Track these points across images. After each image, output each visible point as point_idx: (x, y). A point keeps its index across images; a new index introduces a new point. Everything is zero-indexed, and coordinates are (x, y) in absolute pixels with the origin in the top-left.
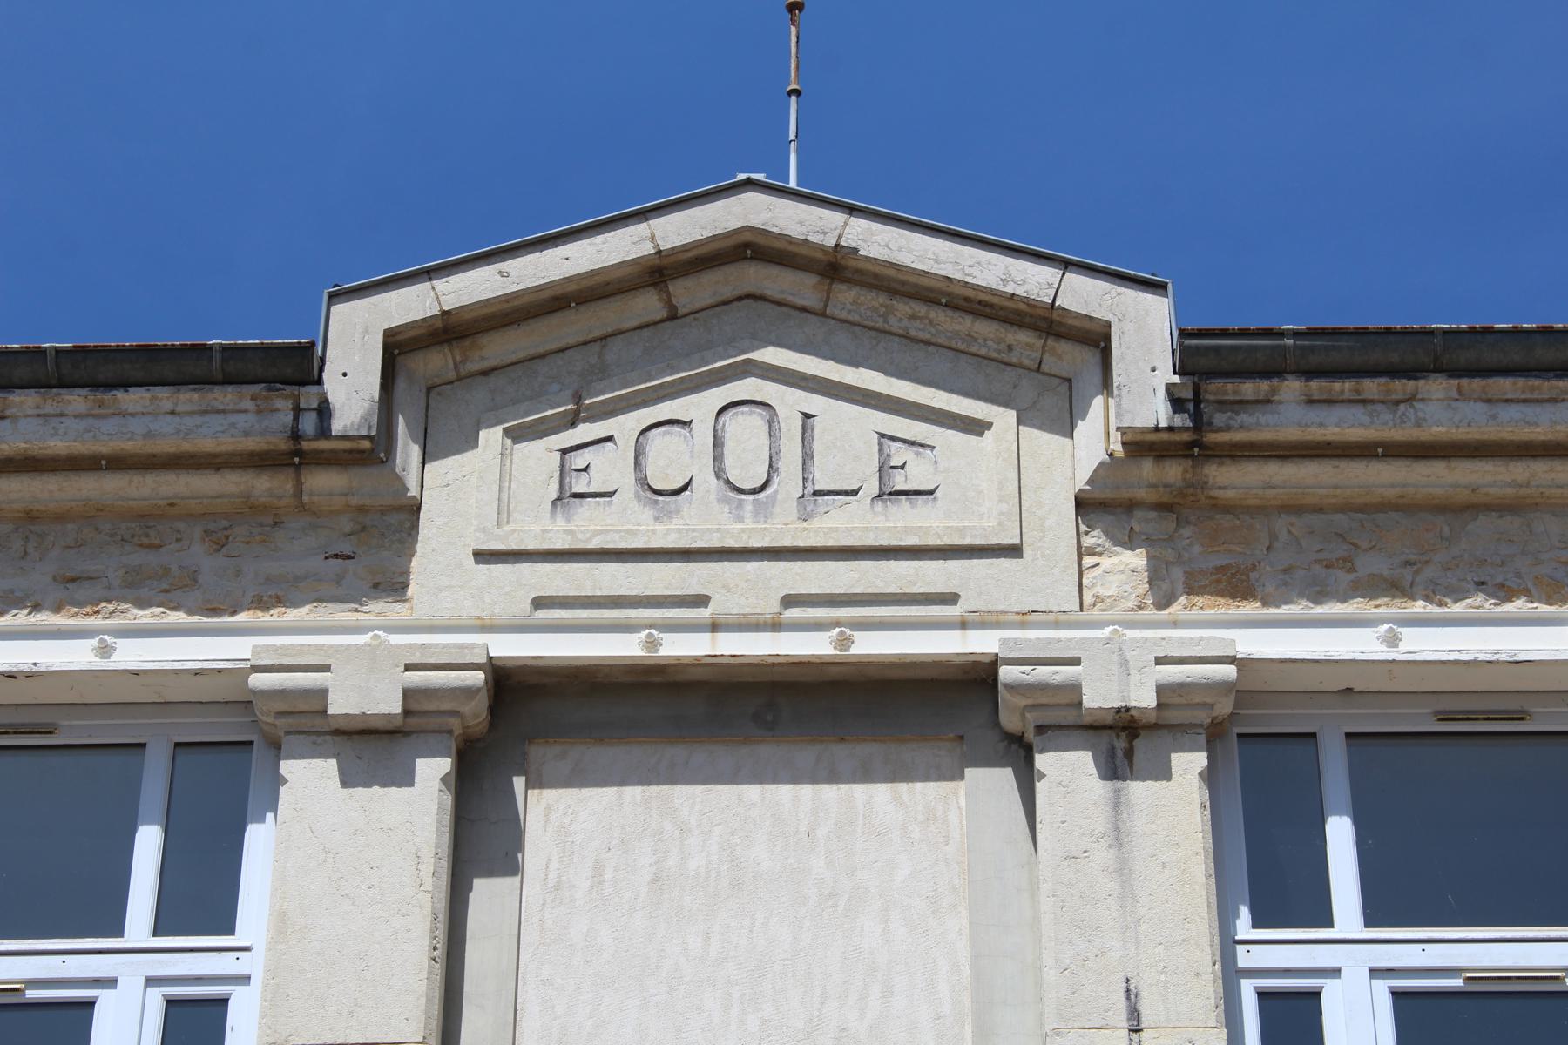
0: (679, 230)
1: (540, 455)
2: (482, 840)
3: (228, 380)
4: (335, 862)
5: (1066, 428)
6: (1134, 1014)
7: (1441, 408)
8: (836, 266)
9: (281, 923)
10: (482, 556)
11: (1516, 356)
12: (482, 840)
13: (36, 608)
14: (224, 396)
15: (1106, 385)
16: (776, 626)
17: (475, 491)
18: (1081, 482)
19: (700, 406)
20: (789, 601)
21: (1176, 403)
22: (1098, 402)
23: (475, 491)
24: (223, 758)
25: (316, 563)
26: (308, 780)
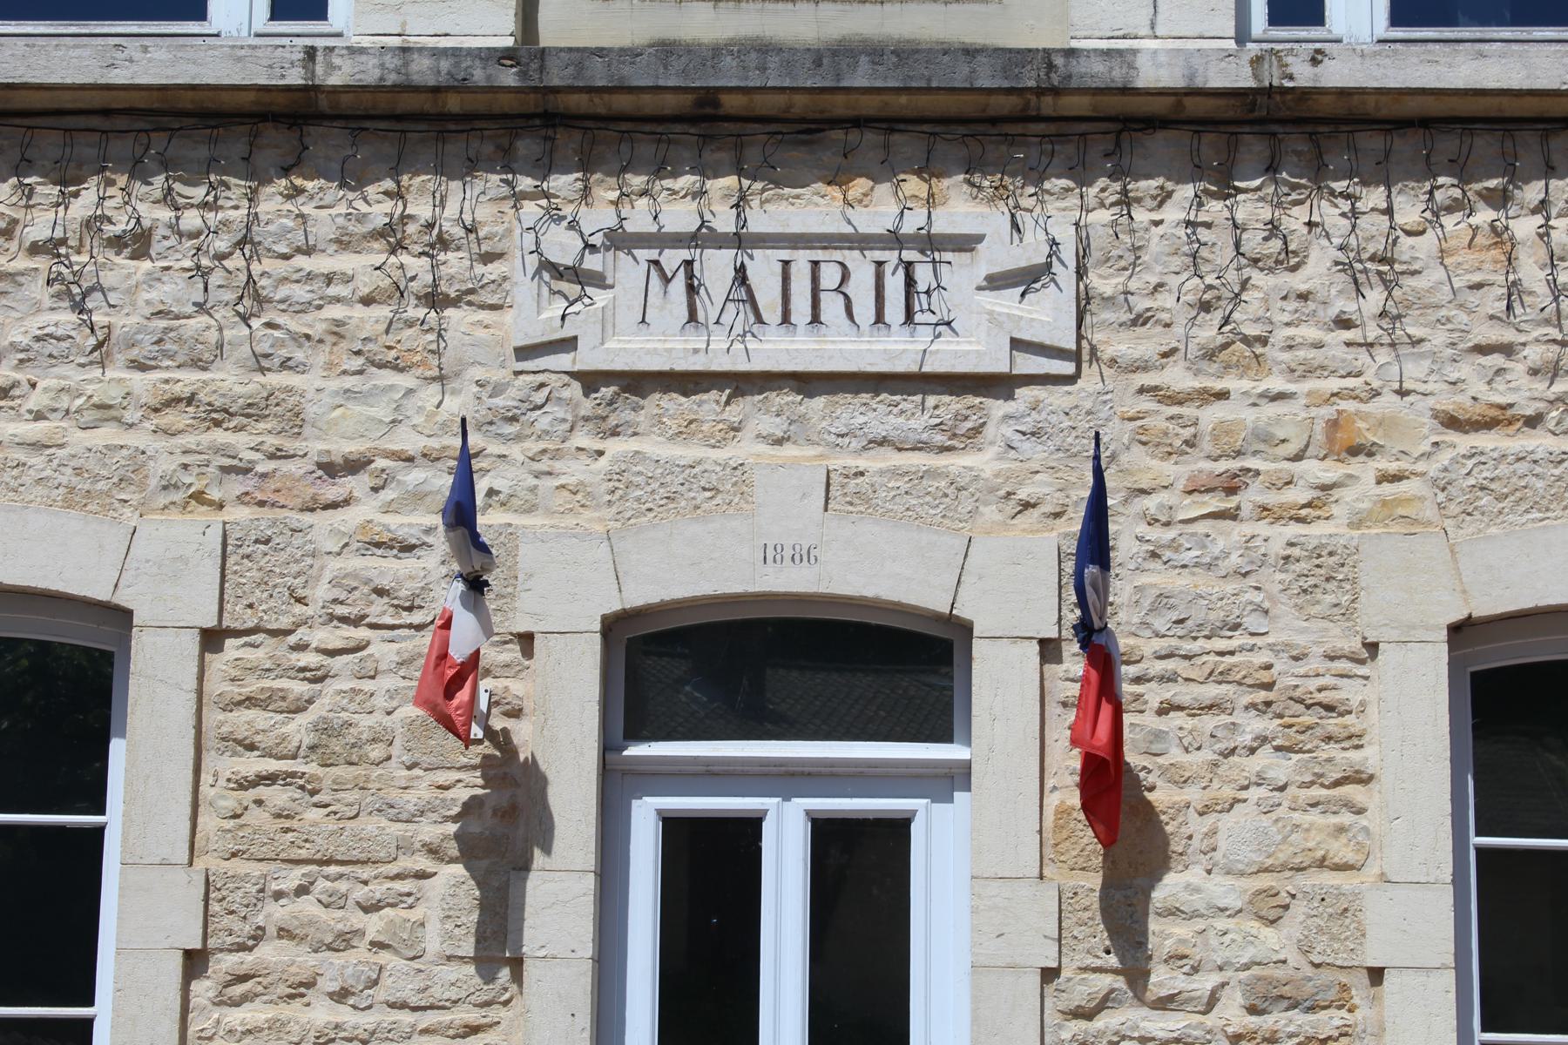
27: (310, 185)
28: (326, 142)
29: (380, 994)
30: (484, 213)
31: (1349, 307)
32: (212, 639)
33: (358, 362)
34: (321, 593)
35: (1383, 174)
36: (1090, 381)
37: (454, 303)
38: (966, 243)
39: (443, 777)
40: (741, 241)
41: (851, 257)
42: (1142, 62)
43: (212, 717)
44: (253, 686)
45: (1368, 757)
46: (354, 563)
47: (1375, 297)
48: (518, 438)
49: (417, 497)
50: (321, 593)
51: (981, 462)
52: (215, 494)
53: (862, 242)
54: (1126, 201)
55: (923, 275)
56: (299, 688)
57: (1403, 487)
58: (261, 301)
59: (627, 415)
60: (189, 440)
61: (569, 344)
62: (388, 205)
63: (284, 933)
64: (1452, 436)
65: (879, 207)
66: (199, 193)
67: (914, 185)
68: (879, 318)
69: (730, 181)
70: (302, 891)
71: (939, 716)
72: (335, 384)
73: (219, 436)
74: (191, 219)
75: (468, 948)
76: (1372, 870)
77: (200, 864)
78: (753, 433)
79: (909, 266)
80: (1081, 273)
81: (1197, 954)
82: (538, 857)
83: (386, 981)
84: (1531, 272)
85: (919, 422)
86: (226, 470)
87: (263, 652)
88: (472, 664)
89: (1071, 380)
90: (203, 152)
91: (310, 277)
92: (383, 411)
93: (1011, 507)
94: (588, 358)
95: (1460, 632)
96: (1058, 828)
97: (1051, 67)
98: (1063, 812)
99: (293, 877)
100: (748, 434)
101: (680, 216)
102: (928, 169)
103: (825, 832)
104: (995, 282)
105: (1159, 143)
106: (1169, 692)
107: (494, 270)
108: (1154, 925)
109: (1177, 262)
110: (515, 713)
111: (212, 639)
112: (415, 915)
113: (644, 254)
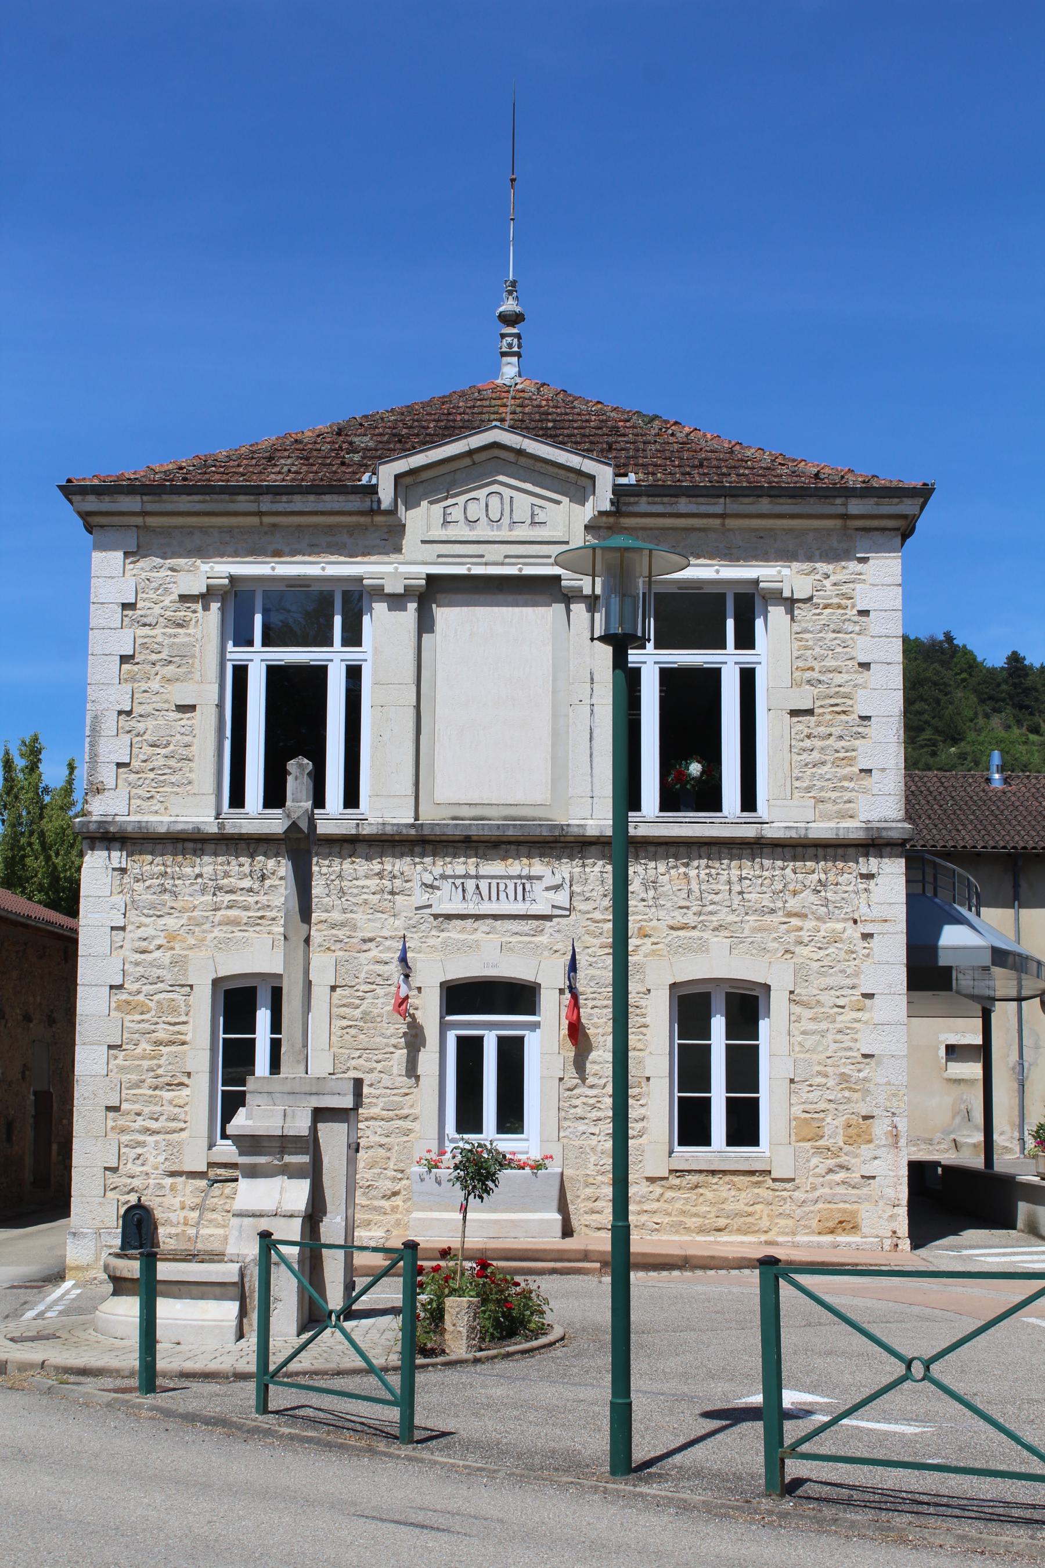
0: (476, 441)
1: (438, 508)
2: (425, 624)
4: (386, 629)
5: (582, 502)
6: (592, 679)
7: (684, 505)
8: (520, 452)
9: (375, 649)
10: (423, 542)
11: (705, 493)
12: (425, 624)
13: (304, 555)
14: (352, 497)
15: (594, 494)
16: (502, 564)
17: (421, 520)
18: (586, 522)
20: (506, 557)
21: (612, 503)
23: (421, 520)
24: (355, 601)
26: (380, 608)
28: (361, 848)
29: (381, 1085)
30: (406, 868)
31: (645, 896)
32: (333, 988)
33: (371, 911)
34: (363, 975)
35: (654, 858)
36: (573, 917)
38: (539, 878)
39: (397, 1026)
40: (477, 877)
41: (508, 881)
42: (588, 828)
43: (334, 1010)
44: (345, 1001)
45: (647, 1020)
46: (372, 967)
47: (651, 893)
48: (416, 932)
49: (389, 949)
52: (333, 948)
53: (511, 877)
54: (584, 866)
55: (528, 887)
56: (358, 1002)
58: (344, 893)
61: (430, 906)
62: (380, 866)
63: (355, 1068)
64: (672, 932)
65: (516, 867)
66: (327, 862)
67: (525, 861)
68: (516, 899)
69: (474, 859)
70: (359, 1057)
71: (532, 1010)
72: (366, 917)
73: (334, 932)
74: (324, 870)
76: (647, 1052)
79: (524, 884)
80: (571, 885)
81: (601, 1074)
84: (694, 886)
87: (347, 992)
88: (407, 997)
89: (568, 916)
90: (327, 851)
91: (358, 887)
92: (378, 925)
93: (552, 952)
95: (673, 986)
99: (357, 1053)
100: (479, 931)
101: (460, 870)
102: (529, 856)
103: (501, 1040)
104: (547, 889)
105: (593, 848)
106: (594, 1003)
107: (408, 885)
108: (588, 1065)
110: (416, 1009)
111: (333, 988)
113: (450, 881)
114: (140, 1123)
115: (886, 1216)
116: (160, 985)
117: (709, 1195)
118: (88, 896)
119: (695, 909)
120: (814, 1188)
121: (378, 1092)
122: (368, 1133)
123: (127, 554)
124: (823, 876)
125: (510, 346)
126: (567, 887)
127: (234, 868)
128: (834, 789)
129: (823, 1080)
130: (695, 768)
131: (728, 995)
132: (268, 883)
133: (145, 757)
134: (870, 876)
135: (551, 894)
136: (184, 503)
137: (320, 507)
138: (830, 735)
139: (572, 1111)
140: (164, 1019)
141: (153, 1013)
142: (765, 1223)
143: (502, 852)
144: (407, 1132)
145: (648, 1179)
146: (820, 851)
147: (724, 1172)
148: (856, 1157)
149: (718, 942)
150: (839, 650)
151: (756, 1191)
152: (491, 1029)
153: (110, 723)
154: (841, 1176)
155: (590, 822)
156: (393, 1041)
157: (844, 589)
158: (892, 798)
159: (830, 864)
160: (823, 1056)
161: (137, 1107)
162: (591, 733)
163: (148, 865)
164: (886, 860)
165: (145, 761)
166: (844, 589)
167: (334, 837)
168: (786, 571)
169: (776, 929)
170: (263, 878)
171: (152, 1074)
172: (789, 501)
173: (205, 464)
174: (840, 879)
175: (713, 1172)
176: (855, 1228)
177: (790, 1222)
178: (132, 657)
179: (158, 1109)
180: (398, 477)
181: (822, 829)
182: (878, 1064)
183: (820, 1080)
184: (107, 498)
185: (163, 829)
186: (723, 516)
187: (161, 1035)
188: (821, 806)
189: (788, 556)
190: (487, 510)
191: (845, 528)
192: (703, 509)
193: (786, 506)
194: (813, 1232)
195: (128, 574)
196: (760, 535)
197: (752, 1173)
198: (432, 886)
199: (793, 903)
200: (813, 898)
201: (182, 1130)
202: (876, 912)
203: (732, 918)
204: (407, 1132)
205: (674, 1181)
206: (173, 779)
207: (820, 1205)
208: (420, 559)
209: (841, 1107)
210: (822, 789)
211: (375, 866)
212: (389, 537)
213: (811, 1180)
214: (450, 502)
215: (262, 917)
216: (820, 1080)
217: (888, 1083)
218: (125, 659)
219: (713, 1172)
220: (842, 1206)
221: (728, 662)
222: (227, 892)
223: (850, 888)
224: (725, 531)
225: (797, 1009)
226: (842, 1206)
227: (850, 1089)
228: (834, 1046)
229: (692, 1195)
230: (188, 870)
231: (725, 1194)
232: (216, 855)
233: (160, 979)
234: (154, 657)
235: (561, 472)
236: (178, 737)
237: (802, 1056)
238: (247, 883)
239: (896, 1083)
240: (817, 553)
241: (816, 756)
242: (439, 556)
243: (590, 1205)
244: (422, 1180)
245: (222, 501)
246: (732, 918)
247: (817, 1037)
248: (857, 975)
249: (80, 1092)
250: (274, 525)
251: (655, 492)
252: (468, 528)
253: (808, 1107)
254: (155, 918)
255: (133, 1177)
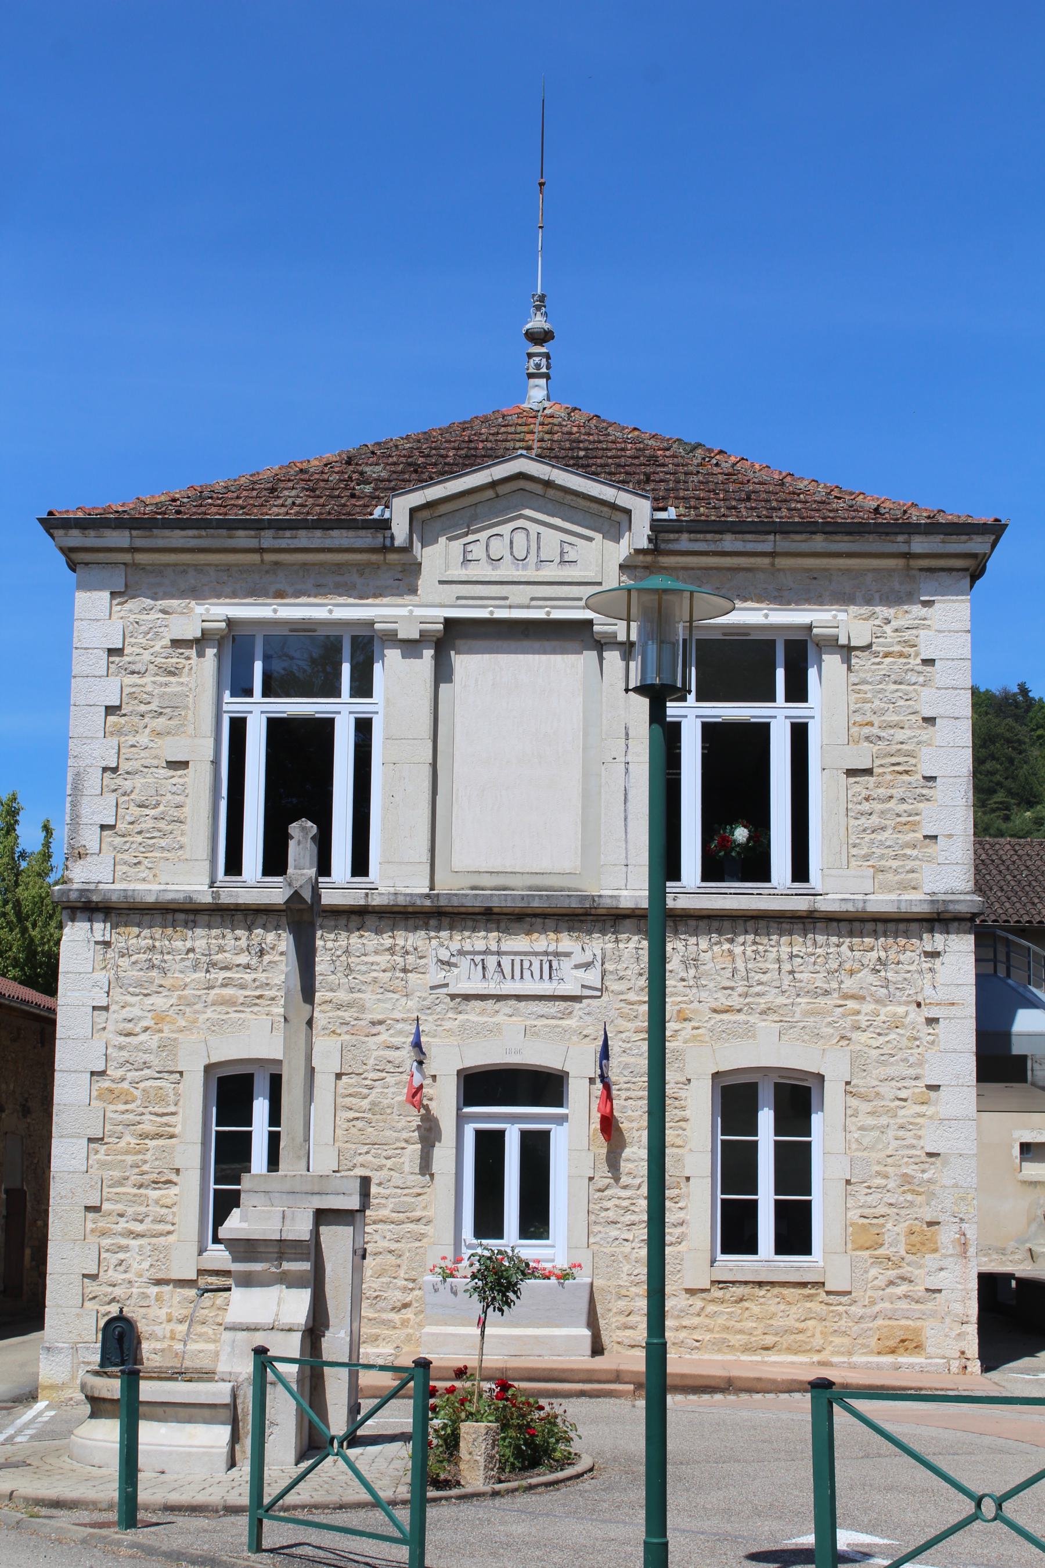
0: (500, 471)
1: (457, 545)
2: (443, 673)
3: (363, 528)
5: (617, 539)
6: (627, 734)
7: (729, 542)
8: (548, 484)
9: (387, 701)
10: (441, 582)
11: (753, 529)
12: (443, 673)
13: (309, 596)
15: (630, 529)
16: (528, 607)
17: (438, 558)
18: (621, 561)
19: (505, 529)
20: (532, 599)
21: (650, 540)
22: (627, 533)
23: (438, 558)
24: (366, 646)
25: (391, 582)
26: (393, 655)
27: (366, 934)
28: (370, 921)
29: (391, 1184)
30: (420, 943)
31: (684, 975)
32: (339, 1076)
34: (371, 1062)
35: (696, 933)
36: (605, 997)
37: (411, 972)
38: (568, 955)
39: (409, 1119)
40: (499, 953)
41: (533, 958)
42: (622, 899)
43: (339, 1100)
44: (351, 1091)
45: (687, 1114)
46: (382, 1053)
47: (692, 972)
48: (431, 1014)
49: (400, 1033)
50: (371, 1062)
51: (571, 1023)
52: (338, 1031)
53: (536, 954)
54: (617, 941)
55: (555, 964)
57: (700, 1031)
59: (464, 1007)
60: (330, 1014)
61: (446, 985)
62: (391, 941)
63: (362, 1165)
65: (542, 942)
66: (332, 936)
67: (552, 935)
68: (541, 977)
69: (496, 934)
70: (367, 1153)
72: (374, 997)
73: (340, 1013)
74: (330, 945)
75: (417, 1170)
76: (688, 1147)
77: (337, 1145)
78: (502, 1015)
81: (635, 1173)
82: (437, 1144)
83: (393, 1180)
84: (740, 964)
85: (555, 1009)
86: (342, 1024)
88: (421, 1087)
89: (600, 997)
90: (333, 923)
91: (366, 963)
93: (581, 1037)
94: (452, 990)
95: (716, 1076)
96: (594, 1135)
97: (594, 901)
98: (595, 1130)
99: (365, 1148)
100: (501, 1013)
101: (480, 945)
102: (556, 931)
103: (525, 1135)
104: (577, 967)
107: (422, 962)
108: (622, 1164)
109: (632, 960)
110: (431, 1099)
111: (339, 1076)
112: (401, 1160)
113: (469, 957)
114: (123, 1225)
115: (953, 1334)
116: (146, 1071)
117: (756, 1309)
118: (67, 973)
119: (740, 990)
120: (873, 1303)
121: (388, 1192)
122: (376, 1237)
123: (113, 594)
124: (883, 954)
125: (538, 366)
126: (598, 964)
127: (229, 942)
128: (895, 857)
129: (883, 1182)
130: (741, 834)
131: (777, 1086)
132: (267, 958)
133: (132, 819)
134: (935, 955)
135: (580, 973)
136: (177, 538)
137: (328, 543)
138: (891, 797)
139: (603, 1214)
140: (150, 1109)
141: (139, 1102)
142: (818, 1341)
143: (526, 926)
144: (420, 1237)
145: (689, 1291)
146: (880, 927)
147: (772, 1284)
148: (920, 1267)
149: (767, 1027)
150: (901, 703)
151: (808, 1305)
152: (513, 1122)
153: (93, 780)
154: (903, 1289)
155: (625, 893)
156: (405, 1135)
157: (907, 635)
158: (959, 868)
159: (891, 940)
160: (883, 1154)
161: (119, 1207)
162: (626, 794)
163: (134, 938)
164: (953, 937)
165: (132, 823)
166: (907, 635)
167: (342, 908)
168: (842, 616)
169: (830, 1013)
170: (262, 953)
171: (137, 1170)
172: (846, 538)
173: (201, 496)
174: (902, 958)
175: (760, 1284)
176: (919, 1347)
177: (846, 1340)
178: (119, 708)
179: (143, 1209)
180: (413, 511)
181: (882, 902)
182: (945, 1163)
183: (879, 1181)
184: (92, 533)
185: (151, 899)
186: (773, 555)
187: (147, 1128)
188: (880, 876)
189: (844, 599)
190: (511, 548)
191: (908, 568)
192: (750, 547)
193: (843, 544)
194: (871, 1352)
195: (115, 616)
196: (814, 576)
197: (804, 1285)
198: (448, 964)
199: (849, 984)
200: (872, 978)
201: (169, 1233)
202: (942, 995)
203: (781, 1000)
204: (420, 1237)
205: (716, 1293)
206: (163, 843)
207: (880, 1322)
208: (437, 601)
209: (903, 1212)
210: (882, 857)
211: (386, 940)
212: (404, 577)
213: (869, 1293)
214: (471, 538)
215: (259, 997)
216: (879, 1181)
217: (956, 1186)
218: (110, 710)
219: (760, 1284)
220: (903, 1322)
221: (778, 716)
222: (221, 969)
223: (912, 968)
224: (774, 570)
225: (854, 1102)
226: (903, 1322)
227: (913, 1192)
228: (895, 1144)
229: (736, 1309)
230: (178, 944)
231: (773, 1309)
232: (210, 927)
233: (146, 1065)
234: (143, 708)
235: (594, 506)
236: (169, 796)
237: (859, 1154)
238: (243, 959)
239: (965, 1185)
240: (877, 596)
241: (875, 820)
242: (458, 598)
243: (623, 1319)
244: (436, 1291)
245: (219, 537)
246: (781, 1000)
247: (876, 1134)
248: (920, 1064)
249: (57, 1190)
250: (276, 563)
251: (697, 527)
252: (490, 567)
253: (867, 1212)
254: (141, 997)
255: (114, 1286)
